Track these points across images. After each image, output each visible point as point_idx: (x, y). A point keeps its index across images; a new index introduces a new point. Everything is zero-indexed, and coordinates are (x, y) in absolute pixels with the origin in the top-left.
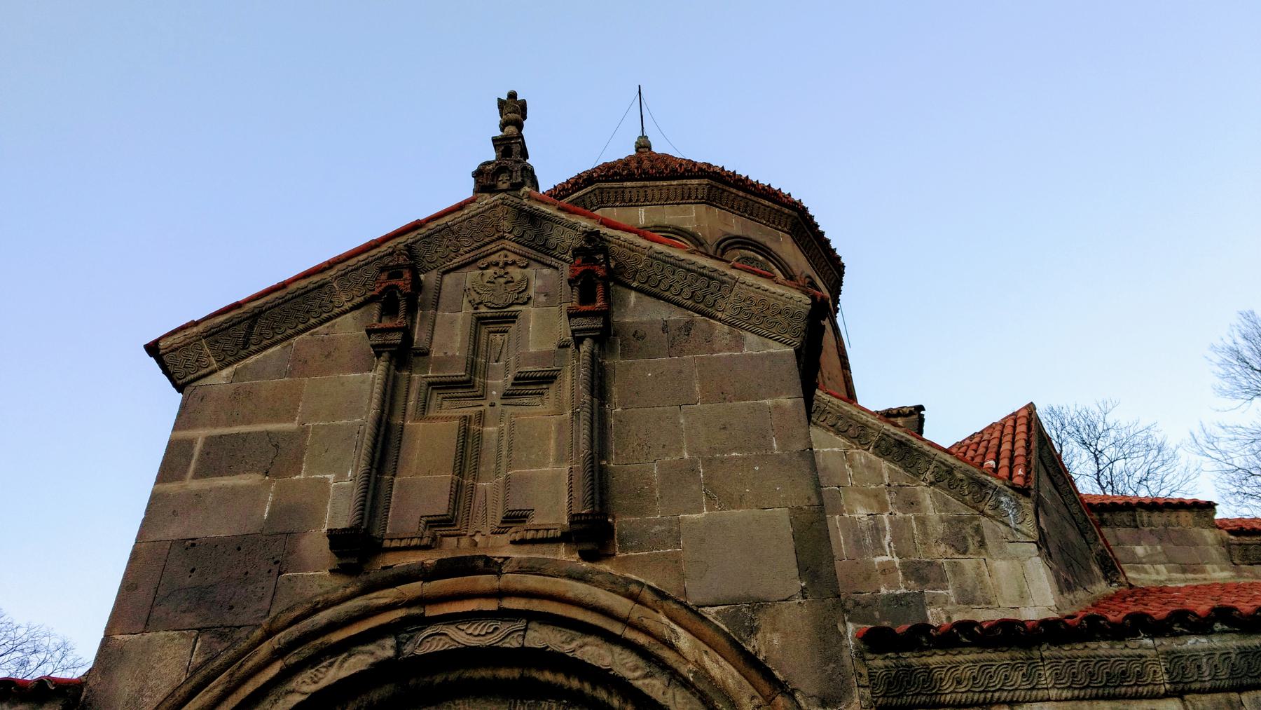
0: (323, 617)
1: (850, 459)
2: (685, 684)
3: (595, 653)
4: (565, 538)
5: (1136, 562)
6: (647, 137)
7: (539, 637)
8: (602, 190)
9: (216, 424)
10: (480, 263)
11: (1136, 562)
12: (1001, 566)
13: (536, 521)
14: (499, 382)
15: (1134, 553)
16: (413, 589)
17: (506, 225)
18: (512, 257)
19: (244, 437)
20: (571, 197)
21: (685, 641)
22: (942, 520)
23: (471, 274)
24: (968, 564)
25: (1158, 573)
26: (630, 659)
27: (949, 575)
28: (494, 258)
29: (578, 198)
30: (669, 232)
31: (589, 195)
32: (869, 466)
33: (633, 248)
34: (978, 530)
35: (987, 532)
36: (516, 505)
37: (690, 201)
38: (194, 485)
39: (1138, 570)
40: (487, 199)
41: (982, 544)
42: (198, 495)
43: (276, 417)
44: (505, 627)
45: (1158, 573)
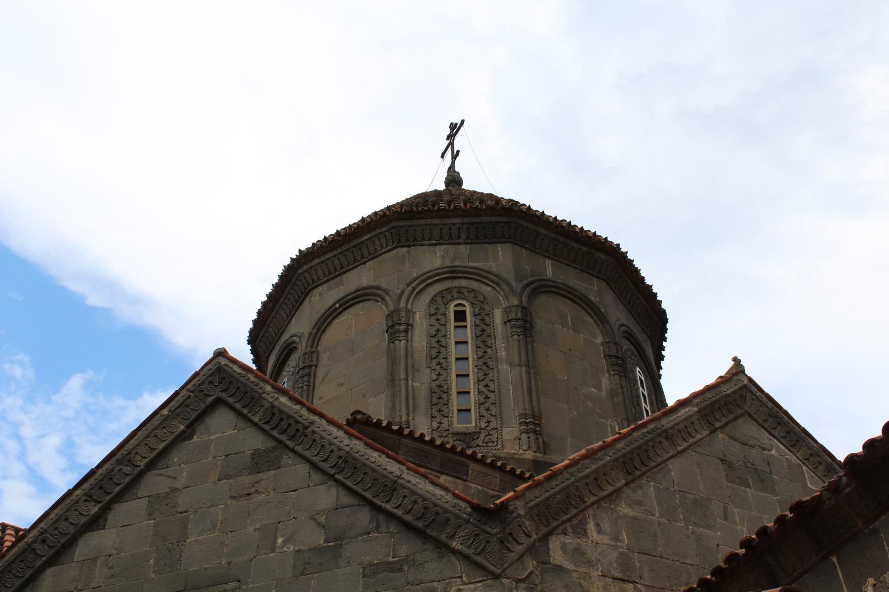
20: (480, 218)
29: (489, 223)
30: (576, 296)
31: (501, 225)
37: (591, 272)
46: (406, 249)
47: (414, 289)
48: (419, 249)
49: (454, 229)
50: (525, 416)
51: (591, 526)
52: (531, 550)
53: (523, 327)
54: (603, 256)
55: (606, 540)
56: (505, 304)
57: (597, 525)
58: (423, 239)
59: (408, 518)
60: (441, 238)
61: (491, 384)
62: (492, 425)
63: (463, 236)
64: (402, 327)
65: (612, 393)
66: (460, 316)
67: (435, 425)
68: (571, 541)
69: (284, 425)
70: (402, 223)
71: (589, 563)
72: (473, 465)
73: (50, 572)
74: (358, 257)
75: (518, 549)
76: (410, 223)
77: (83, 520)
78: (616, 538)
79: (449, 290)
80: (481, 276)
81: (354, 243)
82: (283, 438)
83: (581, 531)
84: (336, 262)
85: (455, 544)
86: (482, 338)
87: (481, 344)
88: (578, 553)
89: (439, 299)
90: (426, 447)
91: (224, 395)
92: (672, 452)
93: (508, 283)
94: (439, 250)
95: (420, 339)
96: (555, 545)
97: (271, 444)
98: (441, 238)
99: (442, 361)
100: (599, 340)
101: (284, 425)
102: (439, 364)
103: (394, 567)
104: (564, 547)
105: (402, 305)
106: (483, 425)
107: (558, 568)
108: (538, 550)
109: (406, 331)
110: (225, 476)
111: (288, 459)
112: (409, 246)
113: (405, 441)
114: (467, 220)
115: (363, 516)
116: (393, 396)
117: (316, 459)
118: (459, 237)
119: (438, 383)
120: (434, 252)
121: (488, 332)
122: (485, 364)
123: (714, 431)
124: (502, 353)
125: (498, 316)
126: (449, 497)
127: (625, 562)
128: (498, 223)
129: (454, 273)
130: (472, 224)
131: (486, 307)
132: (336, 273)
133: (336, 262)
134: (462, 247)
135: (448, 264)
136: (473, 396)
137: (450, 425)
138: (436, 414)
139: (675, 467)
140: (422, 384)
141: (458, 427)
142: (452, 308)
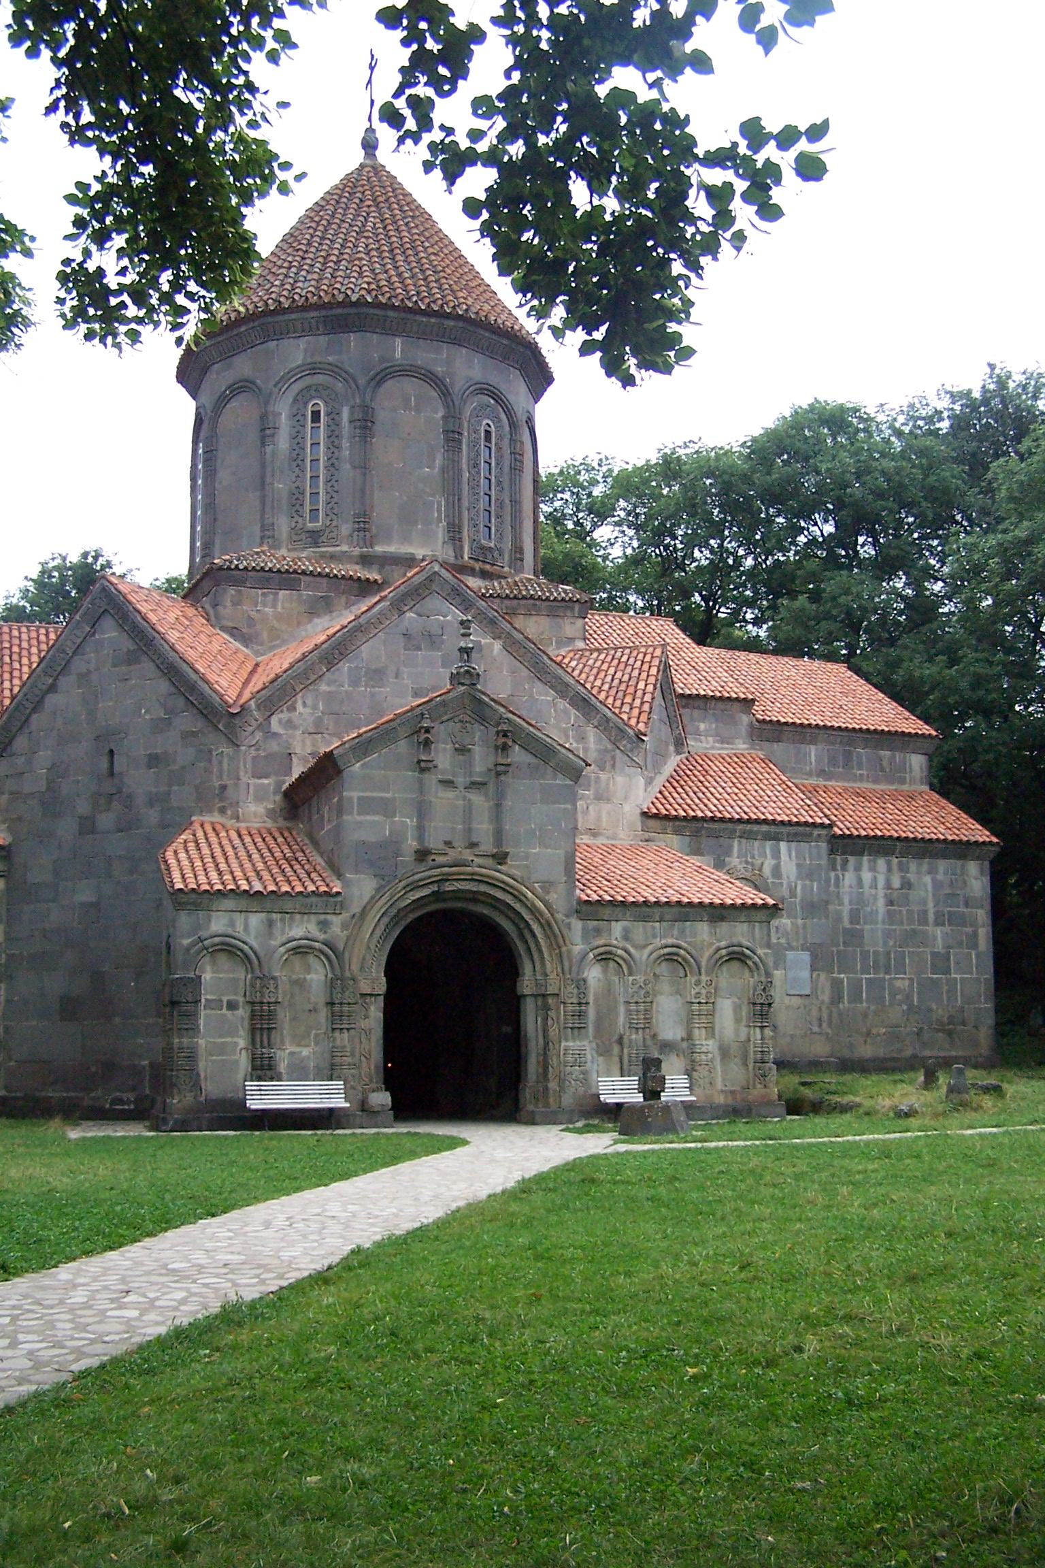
0: (417, 877)
1: (555, 705)
2: (527, 907)
3: (499, 894)
4: (493, 856)
5: (697, 733)
6: (374, 131)
7: (483, 888)
9: (362, 791)
11: (697, 733)
12: (620, 779)
13: (482, 848)
14: (460, 781)
15: (698, 728)
16: (446, 869)
17: (467, 701)
18: (468, 719)
19: (373, 799)
21: (529, 894)
22: (596, 750)
23: (451, 724)
24: (604, 776)
25: (707, 742)
26: (510, 897)
27: (593, 783)
32: (565, 711)
33: (522, 729)
34: (613, 758)
35: (618, 760)
36: (475, 840)
38: (359, 818)
39: (696, 740)
41: (613, 766)
42: (361, 822)
43: (383, 790)
44: (472, 884)
45: (707, 742)
46: (275, 343)
50: (358, 515)
51: (299, 706)
52: (259, 727)
54: (452, 323)
55: (308, 710)
62: (334, 523)
65: (443, 470)
66: (316, 416)
67: (293, 524)
68: (284, 716)
70: (270, 319)
71: (295, 728)
73: (35, 716)
75: (251, 729)
77: (44, 687)
78: (315, 708)
79: (308, 388)
80: (336, 371)
81: (235, 332)
83: (293, 708)
85: (220, 726)
88: (289, 724)
90: (267, 575)
94: (303, 343)
95: (283, 442)
96: (274, 720)
100: (440, 414)
103: (194, 734)
104: (280, 721)
107: (275, 734)
108: (264, 727)
109: (273, 436)
110: (114, 666)
111: (145, 658)
114: (324, 313)
115: (181, 702)
121: (337, 433)
122: (332, 466)
127: (318, 722)
132: (226, 356)
134: (321, 338)
135: (309, 360)
141: (310, 525)
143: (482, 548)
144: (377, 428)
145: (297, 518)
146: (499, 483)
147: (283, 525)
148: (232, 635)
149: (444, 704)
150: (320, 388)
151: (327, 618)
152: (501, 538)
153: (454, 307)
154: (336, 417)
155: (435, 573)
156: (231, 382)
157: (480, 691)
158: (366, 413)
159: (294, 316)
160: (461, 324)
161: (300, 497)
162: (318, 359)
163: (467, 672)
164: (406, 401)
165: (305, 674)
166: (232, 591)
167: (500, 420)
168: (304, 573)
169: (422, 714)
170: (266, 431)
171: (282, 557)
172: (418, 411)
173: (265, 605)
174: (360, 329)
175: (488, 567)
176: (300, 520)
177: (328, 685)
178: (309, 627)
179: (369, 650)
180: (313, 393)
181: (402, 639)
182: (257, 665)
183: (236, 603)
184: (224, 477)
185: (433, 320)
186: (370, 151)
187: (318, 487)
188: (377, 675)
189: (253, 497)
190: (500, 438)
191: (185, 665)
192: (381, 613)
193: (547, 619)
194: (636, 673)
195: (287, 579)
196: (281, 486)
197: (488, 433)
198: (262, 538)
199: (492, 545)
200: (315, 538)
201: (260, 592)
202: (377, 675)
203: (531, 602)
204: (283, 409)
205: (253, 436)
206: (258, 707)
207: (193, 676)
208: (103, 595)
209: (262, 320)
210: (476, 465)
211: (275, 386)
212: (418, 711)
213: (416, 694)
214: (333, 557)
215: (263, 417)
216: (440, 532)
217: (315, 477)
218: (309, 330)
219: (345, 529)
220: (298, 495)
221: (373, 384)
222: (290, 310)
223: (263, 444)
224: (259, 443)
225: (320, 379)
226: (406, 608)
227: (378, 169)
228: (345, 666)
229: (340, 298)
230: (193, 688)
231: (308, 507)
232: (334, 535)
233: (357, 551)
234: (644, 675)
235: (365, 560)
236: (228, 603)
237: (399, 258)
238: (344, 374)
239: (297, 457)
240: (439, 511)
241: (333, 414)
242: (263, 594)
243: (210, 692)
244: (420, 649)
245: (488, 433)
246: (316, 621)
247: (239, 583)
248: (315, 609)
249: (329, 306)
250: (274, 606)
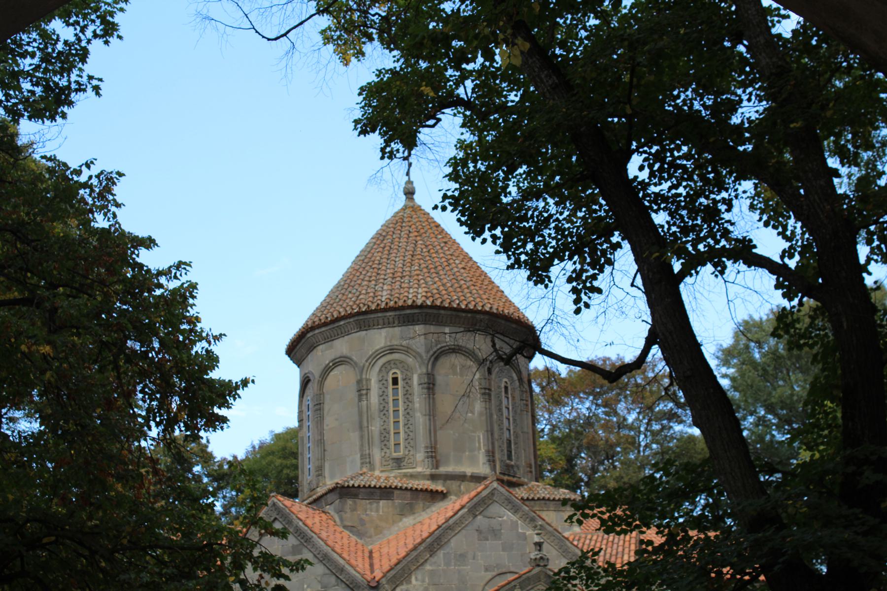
6: (412, 183)
8: (427, 314)
10: (535, 589)
28: (538, 587)
40: (537, 570)
46: (364, 332)
47: (370, 364)
48: (372, 332)
49: (391, 320)
50: (426, 447)
53: (429, 388)
55: (419, 583)
56: (419, 371)
57: (416, 578)
58: (374, 325)
59: (347, 583)
60: (384, 324)
61: (411, 426)
62: (411, 453)
63: (396, 322)
64: (364, 392)
65: (481, 414)
66: (395, 381)
69: (302, 536)
70: (361, 317)
72: (396, 492)
74: (340, 333)
76: (365, 317)
78: (423, 581)
79: (389, 362)
80: (407, 350)
82: (302, 541)
83: (410, 582)
84: (328, 334)
86: (407, 396)
87: (406, 400)
89: (383, 369)
90: (372, 490)
91: (277, 517)
92: (453, 534)
93: (421, 357)
94: (384, 332)
95: (374, 398)
97: (298, 543)
98: (384, 324)
99: (386, 413)
101: (302, 536)
102: (384, 414)
105: (364, 376)
106: (407, 453)
109: (367, 394)
112: (366, 330)
113: (361, 490)
114: (398, 313)
115: (333, 579)
116: (362, 437)
117: (315, 553)
118: (394, 323)
119: (384, 427)
120: (381, 333)
121: (409, 392)
123: (476, 516)
124: (417, 405)
125: (415, 378)
126: (360, 577)
128: (415, 313)
129: (392, 350)
130: (401, 315)
131: (409, 374)
132: (329, 339)
133: (328, 334)
135: (389, 344)
136: (402, 435)
137: (391, 454)
138: (383, 447)
139: (453, 542)
140: (375, 428)
141: (395, 455)
142: (390, 376)
143: (508, 466)
144: (437, 388)
145: (385, 450)
146: (514, 420)
147: (377, 455)
148: (351, 532)
149: (528, 579)
150: (397, 362)
151: (411, 517)
152: (518, 458)
153: (483, 306)
154: (409, 381)
155: (495, 489)
156: (333, 357)
157: (550, 570)
158: (429, 378)
159: (380, 315)
160: (487, 317)
161: (387, 435)
162: (395, 342)
163: (541, 558)
164: (453, 367)
165: (416, 559)
166: (350, 502)
167: (512, 377)
168: (396, 488)
169: (515, 586)
170: (362, 391)
171: (380, 477)
172: (462, 375)
173: (371, 511)
174: (425, 322)
175: (511, 478)
176: (388, 451)
177: (431, 565)
178: (400, 524)
179: (457, 543)
180: (393, 366)
181: (476, 534)
182: (371, 552)
183: (354, 510)
184: (330, 422)
185: (469, 315)
186: (410, 196)
187: (399, 429)
188: (462, 558)
189: (355, 436)
190: (514, 389)
191: (335, 555)
192: (463, 517)
193: (555, 513)
194: (620, 549)
195: (386, 492)
196: (375, 428)
197: (506, 388)
198: (362, 463)
199: (513, 463)
200: (398, 462)
201: (368, 501)
202: (462, 558)
203: (543, 502)
204: (373, 377)
205: (352, 394)
206: (388, 582)
207: (342, 561)
208: (273, 508)
209: (356, 318)
210: (500, 410)
211: (367, 361)
212: (513, 584)
213: (487, 570)
214: (412, 476)
215: (359, 382)
216: (482, 457)
217: (396, 422)
218: (388, 324)
219: (420, 456)
220: (385, 434)
221: (432, 359)
222: (376, 311)
223: (360, 400)
224: (357, 399)
225: (396, 356)
226: (477, 513)
227: (417, 209)
228: (441, 554)
229: (410, 302)
230: (342, 570)
231: (392, 443)
232: (411, 461)
233: (428, 472)
234: (627, 550)
235: (433, 477)
236: (348, 510)
237: (441, 273)
238: (414, 354)
239: (383, 410)
240: (479, 443)
241: (407, 380)
242: (370, 503)
243: (354, 572)
244: (487, 540)
245: (506, 388)
246: (405, 520)
247: (355, 496)
248: (408, 510)
249: (402, 308)
250: (377, 511)
